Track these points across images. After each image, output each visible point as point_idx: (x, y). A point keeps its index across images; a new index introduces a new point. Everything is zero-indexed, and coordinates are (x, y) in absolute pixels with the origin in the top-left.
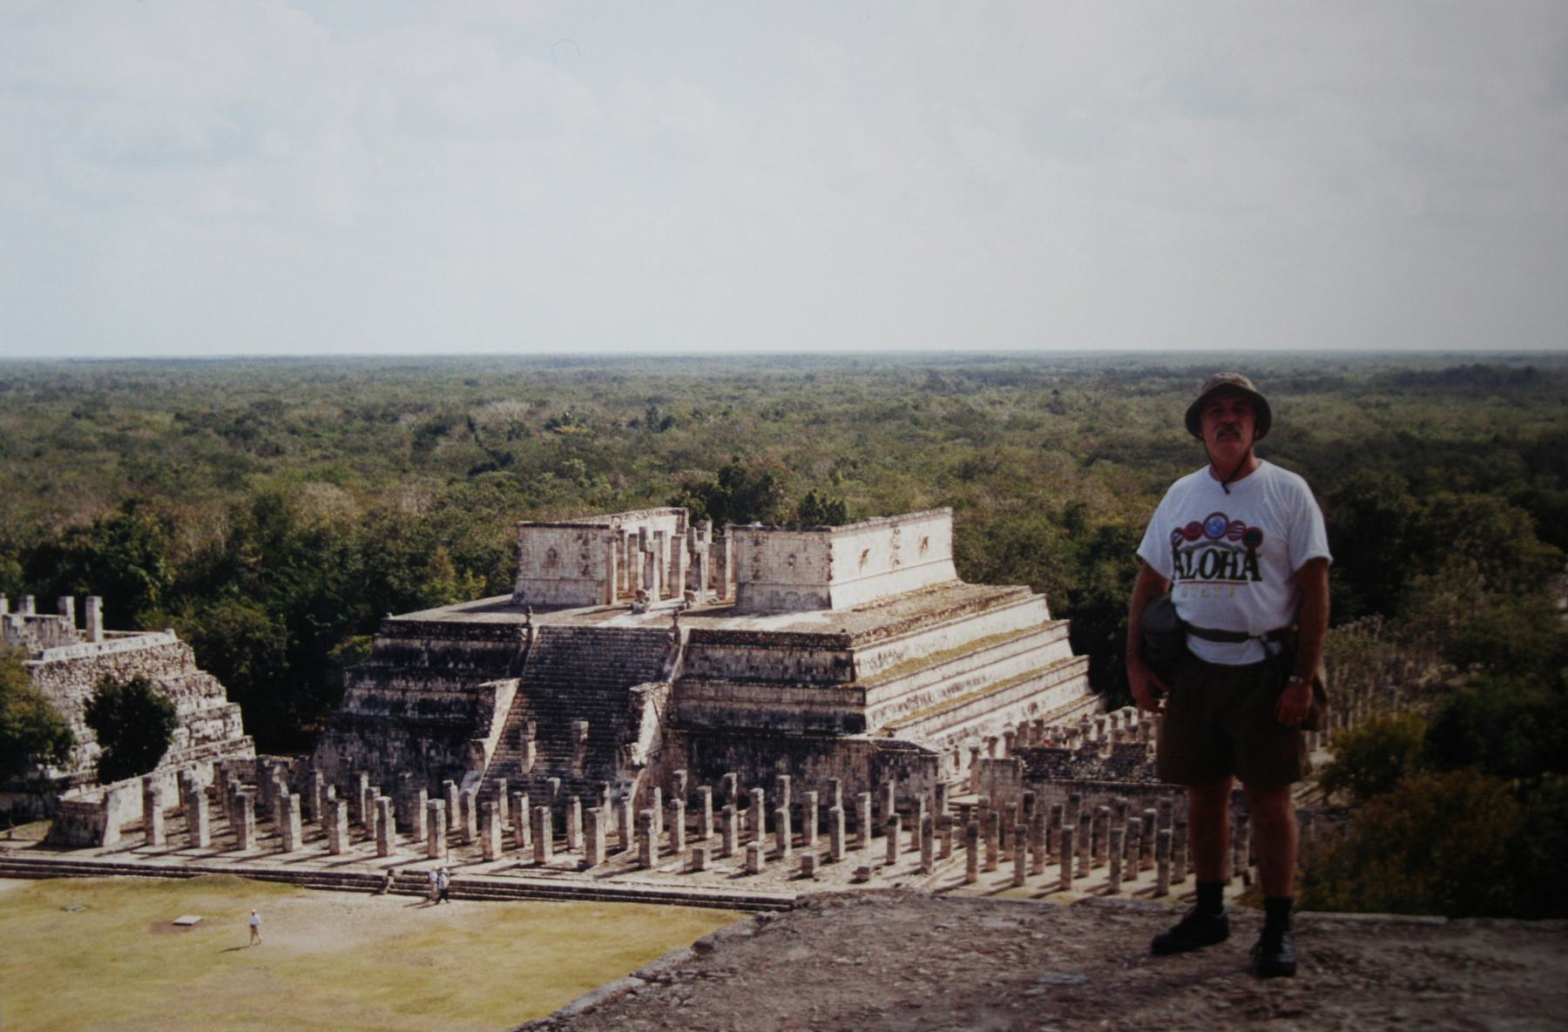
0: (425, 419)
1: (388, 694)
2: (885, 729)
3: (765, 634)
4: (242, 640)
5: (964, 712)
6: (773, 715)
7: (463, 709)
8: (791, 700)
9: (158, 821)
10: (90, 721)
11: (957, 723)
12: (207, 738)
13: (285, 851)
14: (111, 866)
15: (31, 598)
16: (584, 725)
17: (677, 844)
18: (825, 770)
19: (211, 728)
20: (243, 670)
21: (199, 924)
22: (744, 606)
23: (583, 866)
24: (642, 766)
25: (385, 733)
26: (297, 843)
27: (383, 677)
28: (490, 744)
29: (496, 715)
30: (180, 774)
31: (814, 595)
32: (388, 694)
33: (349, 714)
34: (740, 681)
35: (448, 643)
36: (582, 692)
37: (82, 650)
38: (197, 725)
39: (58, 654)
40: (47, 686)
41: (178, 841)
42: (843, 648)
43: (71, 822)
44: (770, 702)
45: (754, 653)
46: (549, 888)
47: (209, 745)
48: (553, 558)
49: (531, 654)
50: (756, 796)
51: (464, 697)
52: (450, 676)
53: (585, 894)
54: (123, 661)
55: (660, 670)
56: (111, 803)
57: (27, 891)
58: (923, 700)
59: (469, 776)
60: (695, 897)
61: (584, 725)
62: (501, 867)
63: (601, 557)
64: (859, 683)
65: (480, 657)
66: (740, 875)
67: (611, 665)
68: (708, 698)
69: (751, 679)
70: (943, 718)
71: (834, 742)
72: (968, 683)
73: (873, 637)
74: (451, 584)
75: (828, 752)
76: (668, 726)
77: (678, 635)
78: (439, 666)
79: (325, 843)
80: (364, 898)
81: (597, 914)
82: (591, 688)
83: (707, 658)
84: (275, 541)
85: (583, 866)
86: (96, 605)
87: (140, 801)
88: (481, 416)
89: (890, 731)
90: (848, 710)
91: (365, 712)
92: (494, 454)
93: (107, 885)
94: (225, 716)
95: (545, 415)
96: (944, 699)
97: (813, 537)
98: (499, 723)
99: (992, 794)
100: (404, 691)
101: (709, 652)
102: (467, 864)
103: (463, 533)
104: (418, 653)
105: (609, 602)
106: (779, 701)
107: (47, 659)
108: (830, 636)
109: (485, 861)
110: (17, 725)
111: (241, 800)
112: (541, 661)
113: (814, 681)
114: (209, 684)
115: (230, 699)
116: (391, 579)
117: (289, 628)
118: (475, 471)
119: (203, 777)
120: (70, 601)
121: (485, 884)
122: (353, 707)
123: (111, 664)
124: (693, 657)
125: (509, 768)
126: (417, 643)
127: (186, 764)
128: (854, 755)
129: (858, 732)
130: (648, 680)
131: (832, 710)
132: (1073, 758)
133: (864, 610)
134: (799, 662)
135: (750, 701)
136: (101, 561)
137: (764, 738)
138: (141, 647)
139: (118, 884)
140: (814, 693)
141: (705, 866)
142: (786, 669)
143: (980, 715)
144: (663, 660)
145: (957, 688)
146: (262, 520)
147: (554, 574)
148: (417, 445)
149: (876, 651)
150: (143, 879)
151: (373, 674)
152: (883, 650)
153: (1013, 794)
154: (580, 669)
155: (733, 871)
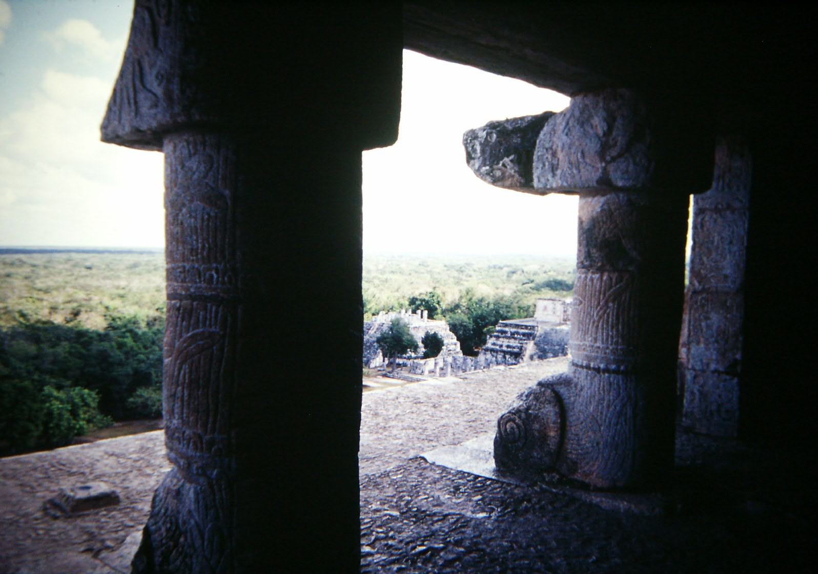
0: (510, 269)
4: (461, 325)
7: (518, 348)
10: (423, 342)
12: (450, 350)
20: (461, 333)
27: (498, 337)
30: (444, 359)
40: (412, 332)
48: (545, 308)
52: (515, 339)
54: (432, 328)
65: (524, 335)
74: (517, 314)
84: (470, 300)
86: (426, 313)
87: (434, 364)
88: (525, 269)
92: (529, 280)
94: (455, 344)
95: (544, 269)
103: (521, 300)
112: (541, 336)
115: (457, 340)
118: (524, 284)
119: (450, 360)
126: (507, 329)
136: (427, 302)
146: (467, 294)
147: (546, 313)
148: (508, 276)
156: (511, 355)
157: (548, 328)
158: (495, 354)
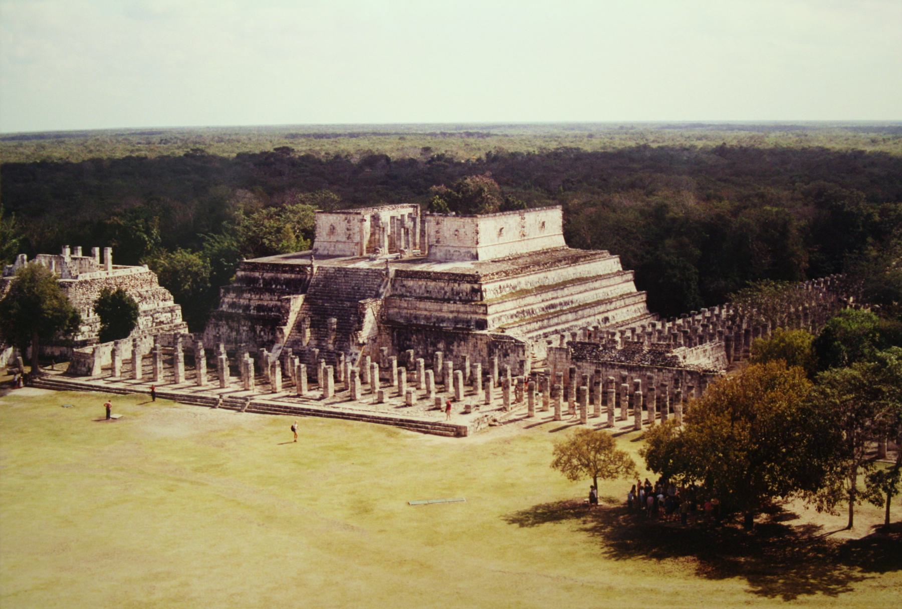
1: (242, 301)
2: (500, 328)
3: (435, 273)
5: (555, 320)
6: (438, 318)
8: (447, 310)
9: (118, 364)
11: (550, 326)
13: (176, 383)
14: (91, 386)
15: (80, 248)
16: (334, 320)
17: (374, 388)
18: (464, 350)
19: (164, 317)
21: (119, 419)
22: (432, 258)
23: (322, 397)
24: (364, 344)
25: (239, 322)
26: (182, 379)
28: (287, 330)
29: (291, 314)
31: (469, 252)
32: (242, 301)
33: (223, 311)
34: (421, 299)
35: (272, 275)
36: (335, 305)
37: (100, 274)
38: (156, 315)
39: (87, 277)
41: (127, 375)
42: (476, 282)
43: (78, 362)
44: (436, 311)
45: (429, 283)
46: (299, 409)
47: (163, 326)
48: (333, 230)
49: (313, 281)
50: (419, 363)
51: (279, 303)
52: (272, 292)
53: (317, 413)
55: (377, 292)
56: (96, 354)
57: (51, 396)
58: (528, 313)
59: (276, 346)
60: (373, 417)
61: (334, 320)
62: (281, 396)
63: (357, 229)
64: (484, 301)
65: (288, 282)
66: (402, 407)
67: (353, 288)
68: (404, 308)
69: (427, 298)
70: (540, 324)
71: (468, 334)
72: (561, 304)
73: (496, 277)
75: (465, 339)
76: (381, 322)
77: (387, 273)
78: (268, 287)
79: (196, 380)
80: (206, 410)
81: (321, 424)
82: (341, 300)
83: (404, 286)
85: (322, 397)
89: (503, 330)
90: (478, 317)
91: (230, 311)
93: (88, 396)
96: (543, 313)
97: (468, 220)
98: (292, 318)
99: (555, 367)
100: (250, 300)
101: (405, 283)
102: (263, 394)
104: (258, 279)
105: (361, 254)
106: (441, 310)
107: (80, 278)
108: (470, 275)
109: (273, 393)
110: (50, 312)
111: (165, 353)
112: (317, 285)
113: (460, 300)
114: (164, 294)
115: (175, 302)
116: (265, 240)
117: (212, 266)
120: (97, 250)
121: (267, 405)
122: (225, 307)
123: (113, 282)
124: (397, 285)
125: (295, 343)
126: (257, 274)
127: (144, 337)
128: (479, 342)
129: (483, 329)
130: (370, 297)
131: (469, 317)
132: (601, 348)
133: (499, 261)
134: (452, 289)
135: (426, 310)
137: (431, 330)
138: (129, 273)
139: (92, 395)
140: (460, 306)
141: (384, 400)
142: (446, 293)
143: (567, 322)
144: (380, 286)
145: (553, 306)
149: (497, 284)
150: (105, 394)
151: (235, 290)
152: (503, 284)
153: (565, 365)
154: (337, 290)
155: (399, 404)
156: (265, 325)
157: (330, 264)
158: (235, 325)
